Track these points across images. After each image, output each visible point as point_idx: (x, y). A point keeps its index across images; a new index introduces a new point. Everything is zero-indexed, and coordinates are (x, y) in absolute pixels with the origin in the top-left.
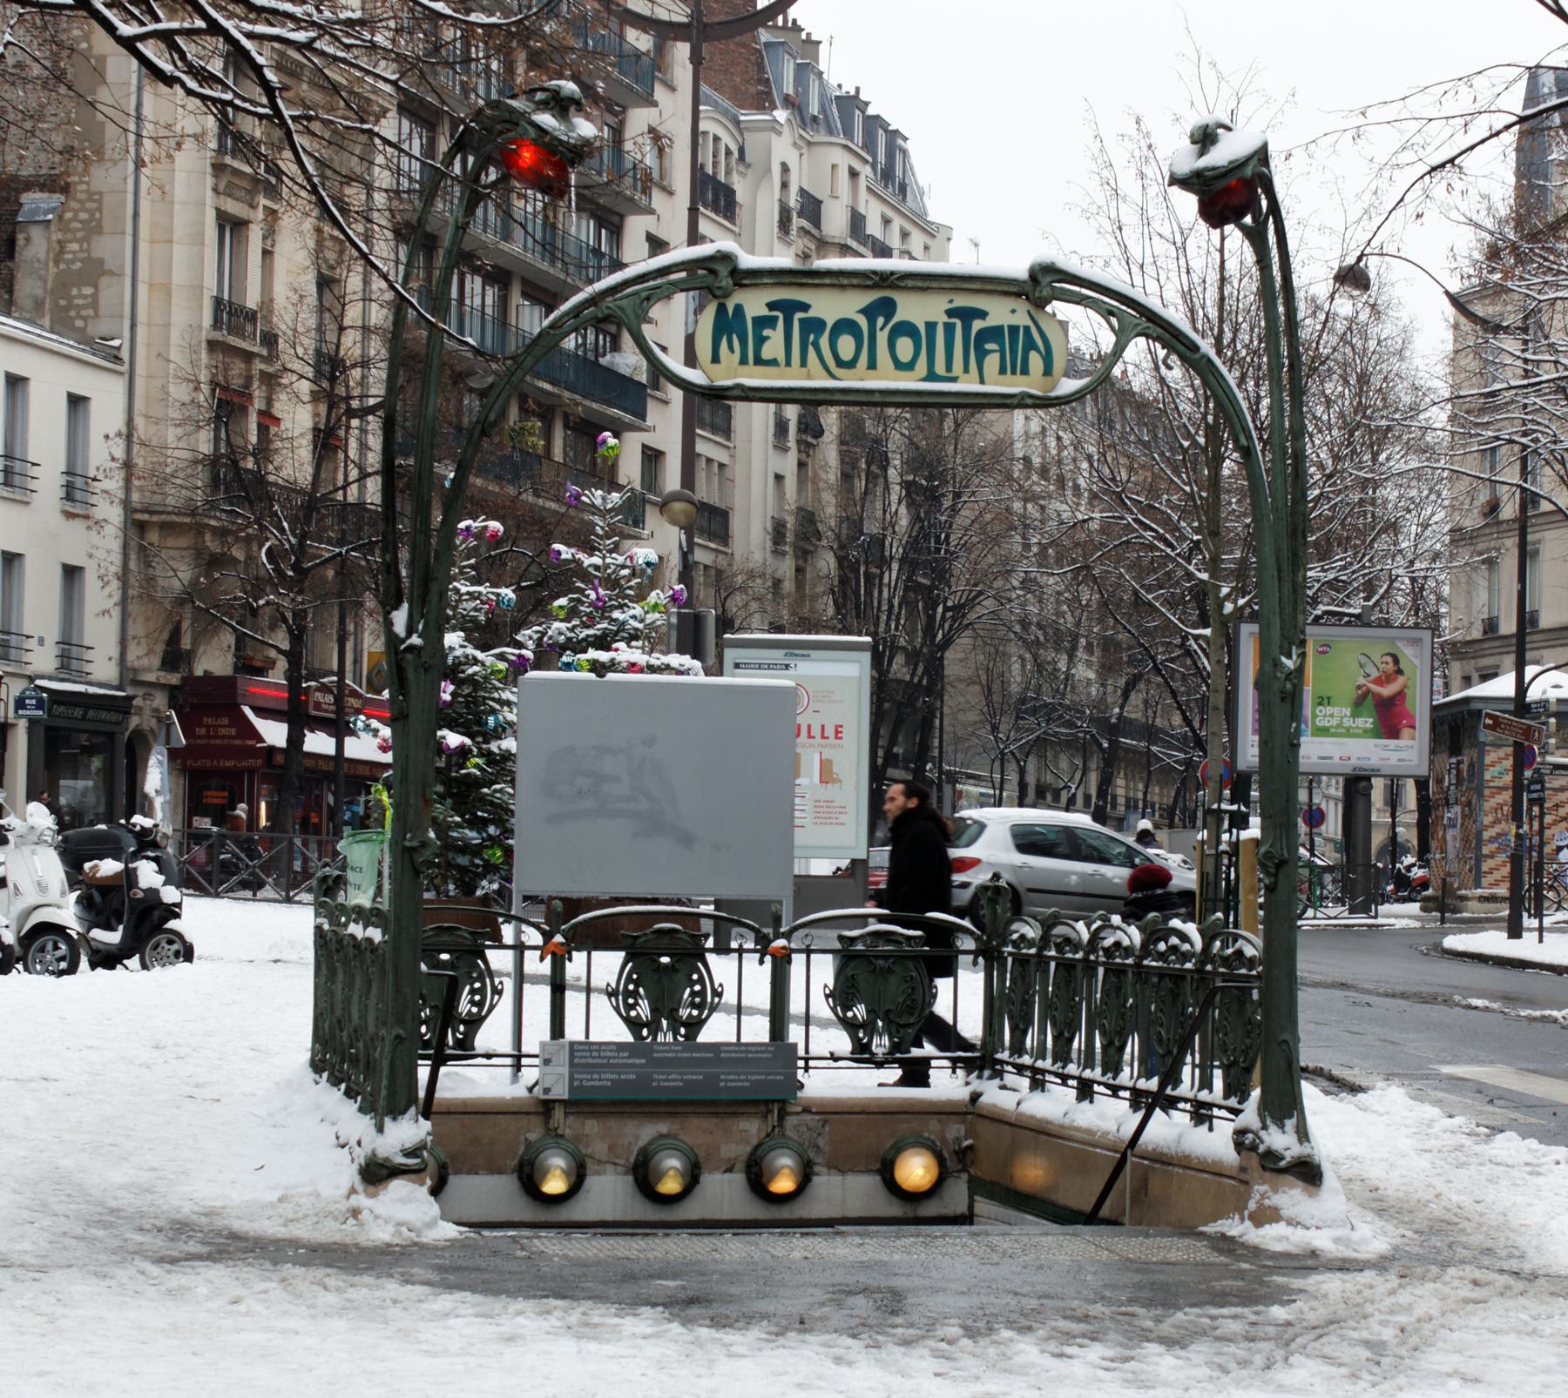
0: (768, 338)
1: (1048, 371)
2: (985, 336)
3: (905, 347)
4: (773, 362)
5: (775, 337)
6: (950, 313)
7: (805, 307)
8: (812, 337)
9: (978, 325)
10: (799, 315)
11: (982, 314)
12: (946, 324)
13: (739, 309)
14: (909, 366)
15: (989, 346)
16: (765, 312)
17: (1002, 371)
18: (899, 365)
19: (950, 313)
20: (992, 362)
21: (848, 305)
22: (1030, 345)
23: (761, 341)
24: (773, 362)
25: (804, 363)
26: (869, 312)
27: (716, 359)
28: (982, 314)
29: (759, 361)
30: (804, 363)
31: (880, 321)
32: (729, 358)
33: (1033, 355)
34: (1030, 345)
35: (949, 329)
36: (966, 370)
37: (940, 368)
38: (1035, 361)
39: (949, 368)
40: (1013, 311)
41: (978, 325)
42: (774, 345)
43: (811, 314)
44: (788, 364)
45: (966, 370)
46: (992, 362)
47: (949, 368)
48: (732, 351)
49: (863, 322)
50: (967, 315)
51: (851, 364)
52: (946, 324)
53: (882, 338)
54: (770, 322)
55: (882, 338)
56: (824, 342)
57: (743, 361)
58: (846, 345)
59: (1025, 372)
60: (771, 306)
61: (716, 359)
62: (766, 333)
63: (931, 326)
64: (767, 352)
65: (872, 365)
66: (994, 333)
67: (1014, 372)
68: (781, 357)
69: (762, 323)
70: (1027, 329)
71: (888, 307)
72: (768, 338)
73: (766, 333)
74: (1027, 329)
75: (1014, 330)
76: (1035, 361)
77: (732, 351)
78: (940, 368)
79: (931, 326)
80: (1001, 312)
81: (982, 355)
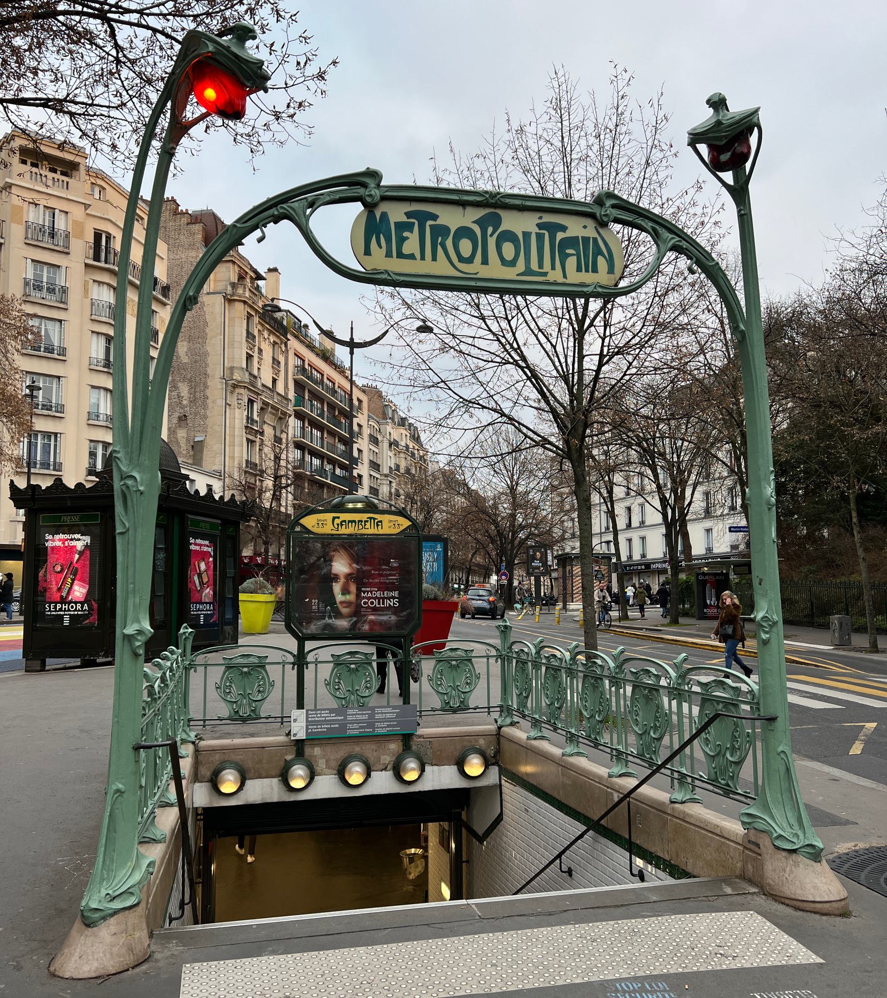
0: (407, 238)
1: (611, 270)
3: (508, 249)
4: (412, 257)
6: (540, 226)
7: (435, 217)
8: (440, 239)
9: (560, 236)
10: (430, 223)
11: (564, 229)
12: (536, 233)
13: (384, 215)
14: (513, 263)
15: (568, 251)
16: (404, 219)
17: (579, 269)
18: (504, 262)
21: (468, 218)
22: (598, 252)
23: (401, 240)
24: (412, 257)
25: (434, 258)
28: (564, 229)
29: (400, 255)
30: (434, 258)
31: (490, 230)
33: (600, 259)
34: (598, 252)
35: (540, 237)
36: (553, 268)
37: (534, 266)
39: (541, 266)
40: (585, 227)
41: (560, 236)
42: (411, 245)
43: (439, 222)
44: (423, 258)
45: (553, 268)
47: (541, 266)
48: (380, 247)
50: (553, 228)
51: (470, 260)
52: (536, 233)
53: (492, 242)
54: (409, 227)
55: (492, 242)
56: (449, 243)
57: (389, 255)
58: (466, 247)
59: (595, 270)
60: (408, 215)
62: (405, 234)
63: (526, 235)
64: (407, 249)
65: (485, 261)
66: (572, 242)
67: (587, 271)
68: (418, 255)
69: (402, 227)
70: (595, 239)
71: (496, 221)
72: (407, 238)
73: (405, 234)
74: (595, 239)
75: (586, 240)
76: (602, 262)
77: (380, 247)
78: (534, 266)
80: (576, 228)
81: (564, 258)
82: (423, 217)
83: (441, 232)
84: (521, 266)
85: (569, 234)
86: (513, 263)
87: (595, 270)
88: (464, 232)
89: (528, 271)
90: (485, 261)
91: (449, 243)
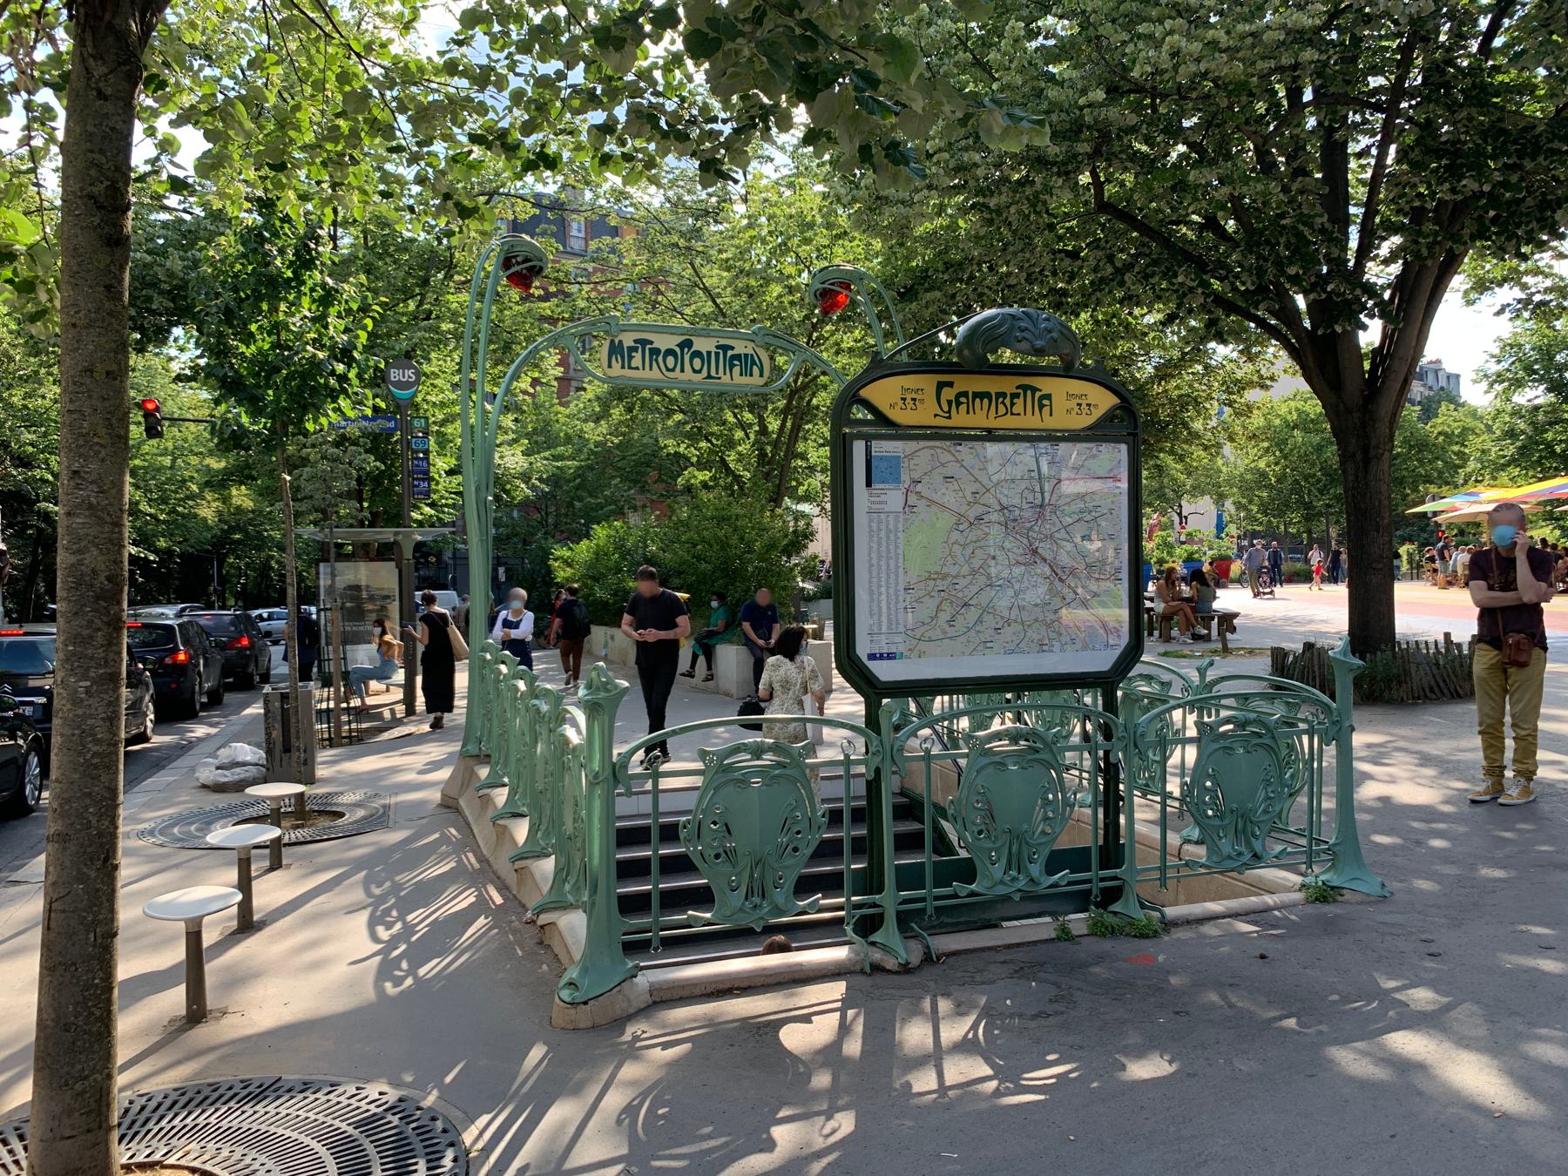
2: (734, 357)
3: (697, 363)
5: (638, 356)
9: (730, 353)
11: (732, 348)
20: (737, 370)
23: (631, 358)
26: (682, 345)
27: (610, 366)
28: (732, 348)
32: (616, 365)
34: (753, 363)
35: (717, 354)
37: (713, 373)
38: (756, 370)
41: (730, 353)
42: (637, 361)
46: (737, 370)
49: (678, 350)
50: (725, 348)
51: (673, 370)
53: (687, 358)
54: (636, 349)
55: (687, 358)
56: (660, 359)
58: (670, 361)
61: (610, 366)
63: (709, 353)
65: (682, 371)
66: (738, 357)
69: (632, 349)
76: (756, 370)
79: (709, 353)
81: (732, 366)
82: (644, 342)
83: (655, 352)
84: (705, 373)
85: (735, 352)
86: (700, 371)
88: (670, 352)
89: (709, 377)
90: (682, 371)
91: (660, 359)
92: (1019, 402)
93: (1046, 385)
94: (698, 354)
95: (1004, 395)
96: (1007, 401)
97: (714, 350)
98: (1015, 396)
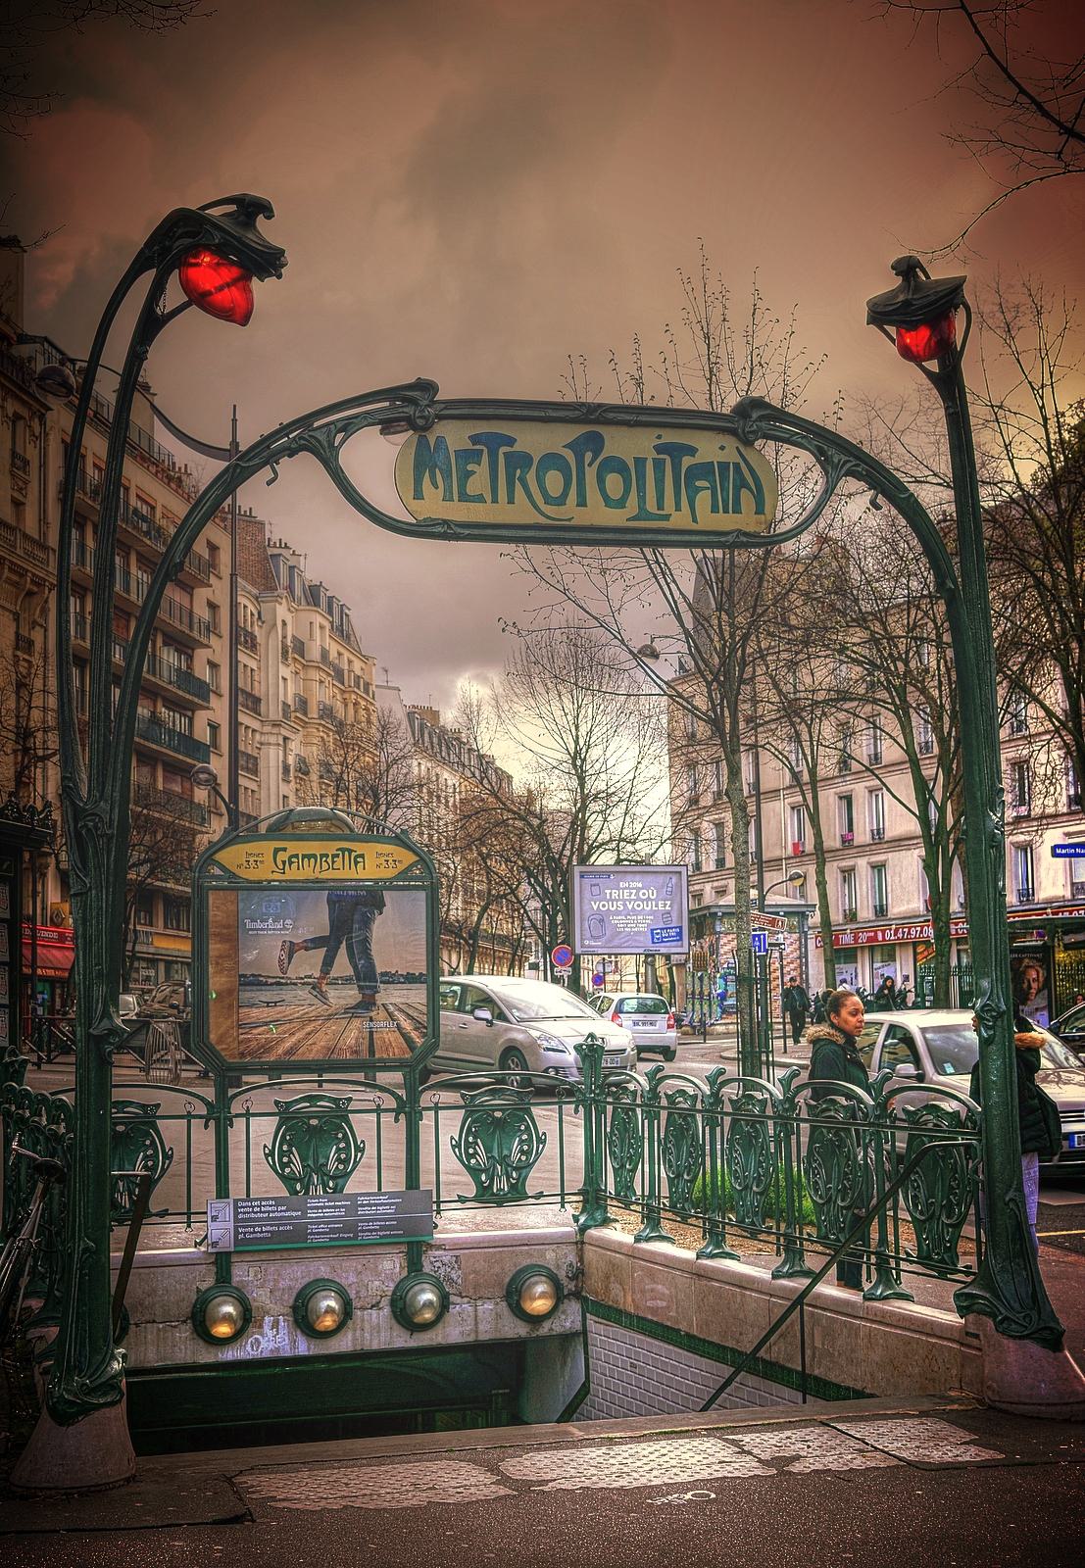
3: (614, 482)
5: (481, 472)
6: (659, 449)
7: (511, 441)
9: (687, 461)
17: (714, 509)
19: (659, 449)
20: (703, 499)
29: (464, 497)
31: (589, 456)
33: (744, 492)
35: (659, 465)
37: (651, 506)
42: (478, 483)
43: (517, 447)
46: (703, 499)
53: (591, 474)
55: (591, 474)
56: (531, 477)
59: (737, 510)
63: (640, 462)
65: (582, 502)
66: (705, 470)
70: (737, 466)
74: (737, 466)
75: (724, 467)
85: (698, 459)
86: (621, 503)
87: (737, 510)
88: (552, 460)
90: (582, 502)
91: (531, 477)
92: (339, 860)
93: (358, 847)
94: (616, 465)
95: (327, 856)
96: (330, 860)
97: (651, 455)
98: (334, 856)
